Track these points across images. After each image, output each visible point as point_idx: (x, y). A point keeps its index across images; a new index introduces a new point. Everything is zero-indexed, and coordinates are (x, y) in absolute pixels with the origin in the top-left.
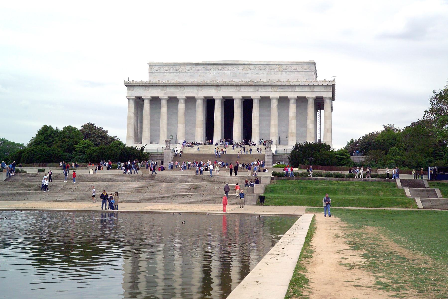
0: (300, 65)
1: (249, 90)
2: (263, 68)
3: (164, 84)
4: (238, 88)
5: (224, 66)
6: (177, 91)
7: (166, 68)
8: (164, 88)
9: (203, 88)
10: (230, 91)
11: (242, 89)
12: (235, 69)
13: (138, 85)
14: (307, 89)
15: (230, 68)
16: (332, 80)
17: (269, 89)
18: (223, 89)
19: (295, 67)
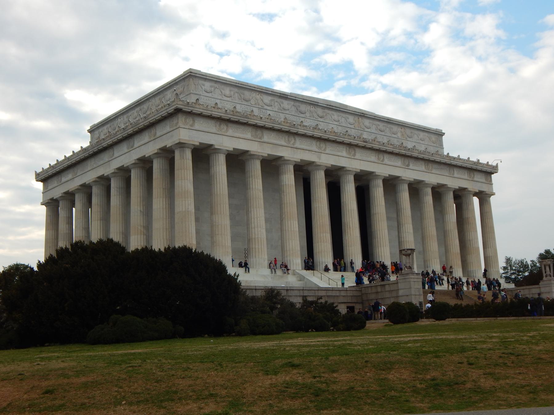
0: (426, 134)
1: (396, 164)
2: (383, 128)
3: (260, 123)
4: (381, 156)
5: (326, 111)
6: (283, 143)
7: (227, 91)
8: (259, 132)
9: (328, 144)
10: (369, 159)
11: (387, 159)
12: (343, 120)
13: (208, 113)
14: (465, 175)
15: (336, 115)
16: (494, 164)
17: (421, 166)
18: (359, 154)
19: (422, 135)
